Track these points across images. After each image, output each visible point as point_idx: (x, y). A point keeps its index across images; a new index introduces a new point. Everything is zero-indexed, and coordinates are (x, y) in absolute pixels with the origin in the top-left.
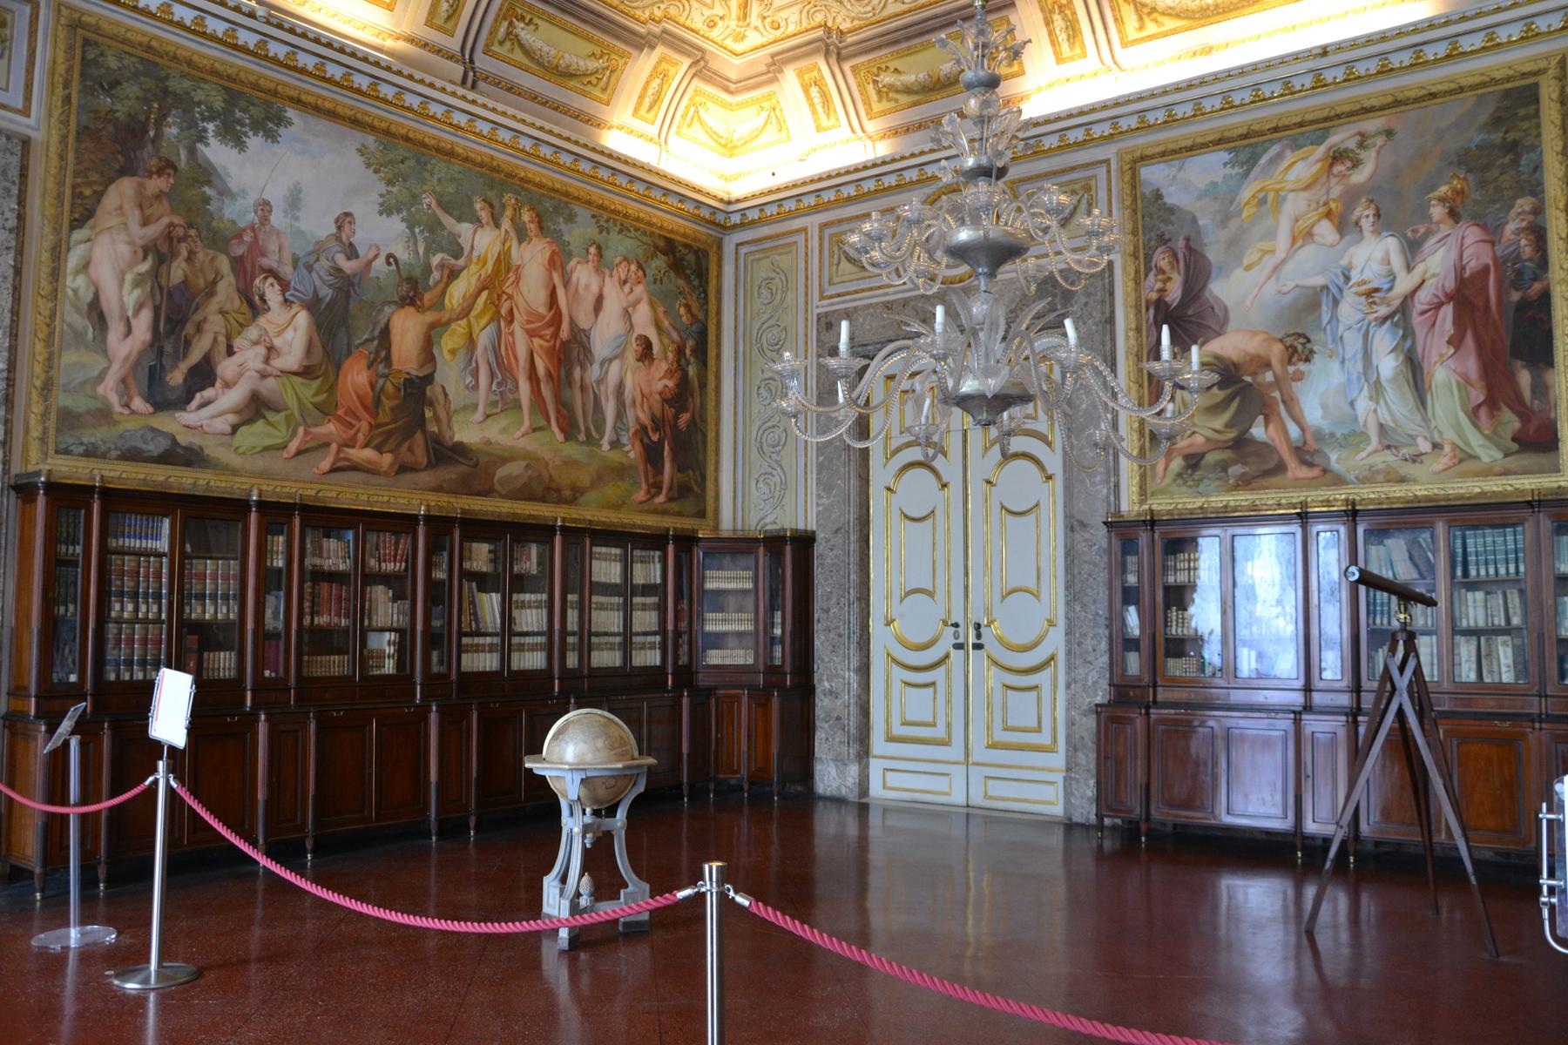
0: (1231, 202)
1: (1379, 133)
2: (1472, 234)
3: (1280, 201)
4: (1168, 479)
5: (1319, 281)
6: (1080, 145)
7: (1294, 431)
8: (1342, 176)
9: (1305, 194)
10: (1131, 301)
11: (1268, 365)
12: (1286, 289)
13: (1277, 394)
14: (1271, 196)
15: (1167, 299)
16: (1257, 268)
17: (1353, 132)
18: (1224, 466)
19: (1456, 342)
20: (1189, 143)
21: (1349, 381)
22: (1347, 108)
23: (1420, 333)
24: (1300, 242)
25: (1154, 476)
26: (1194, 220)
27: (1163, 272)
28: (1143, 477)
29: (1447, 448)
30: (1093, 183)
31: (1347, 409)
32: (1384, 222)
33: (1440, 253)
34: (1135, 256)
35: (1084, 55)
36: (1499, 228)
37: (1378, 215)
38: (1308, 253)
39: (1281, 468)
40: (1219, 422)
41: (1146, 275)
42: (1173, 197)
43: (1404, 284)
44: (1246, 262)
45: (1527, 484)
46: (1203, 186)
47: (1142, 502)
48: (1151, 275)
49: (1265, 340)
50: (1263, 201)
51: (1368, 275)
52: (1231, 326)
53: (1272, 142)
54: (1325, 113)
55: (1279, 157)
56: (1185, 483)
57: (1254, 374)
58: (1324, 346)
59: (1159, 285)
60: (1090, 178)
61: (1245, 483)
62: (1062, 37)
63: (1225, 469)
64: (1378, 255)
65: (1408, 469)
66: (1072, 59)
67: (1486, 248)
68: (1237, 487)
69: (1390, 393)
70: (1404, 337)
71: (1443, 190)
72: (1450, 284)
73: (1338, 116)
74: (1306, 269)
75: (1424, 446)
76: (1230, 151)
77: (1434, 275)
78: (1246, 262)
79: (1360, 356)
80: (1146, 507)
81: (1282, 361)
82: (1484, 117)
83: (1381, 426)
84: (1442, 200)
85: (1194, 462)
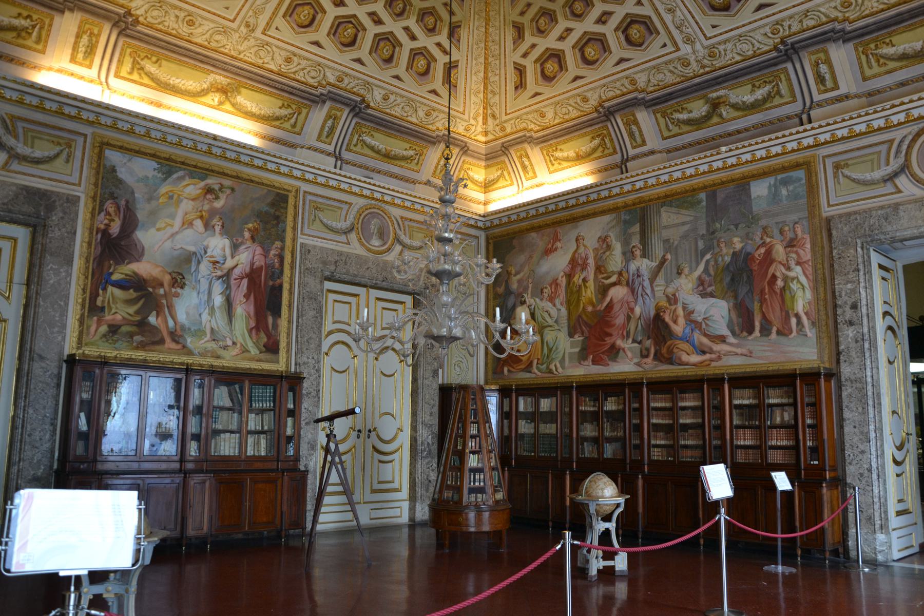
0: (155, 191)
2: (259, 250)
3: (179, 201)
4: (97, 337)
5: (192, 249)
6: (70, 117)
7: (171, 323)
8: (210, 201)
9: (191, 202)
10: (88, 225)
11: (162, 285)
12: (176, 248)
13: (164, 302)
14: (175, 197)
18: (131, 335)
19: (247, 296)
20: (137, 149)
23: (234, 288)
25: (88, 334)
26: (133, 193)
27: (110, 215)
29: (239, 345)
30: (73, 144)
32: (226, 231)
33: (246, 254)
34: (94, 198)
35: (90, 67)
37: (223, 226)
38: (189, 232)
39: (162, 341)
40: (132, 310)
41: (99, 213)
42: (122, 174)
43: (230, 263)
44: (158, 226)
46: (140, 176)
47: (78, 348)
48: (102, 214)
50: (171, 198)
51: (215, 253)
52: (145, 258)
53: (181, 169)
54: (207, 167)
55: (182, 178)
56: (107, 341)
57: (154, 288)
59: (106, 221)
60: (73, 140)
61: (142, 346)
62: (82, 49)
63: (132, 337)
64: (220, 246)
65: (221, 352)
66: (81, 64)
67: (263, 258)
68: (137, 348)
69: (218, 314)
70: (227, 288)
71: (250, 225)
72: (248, 270)
73: (212, 171)
74: (188, 240)
75: (229, 343)
76: (159, 163)
79: (206, 292)
80: (81, 351)
82: (270, 199)
84: (249, 230)
85: (114, 329)
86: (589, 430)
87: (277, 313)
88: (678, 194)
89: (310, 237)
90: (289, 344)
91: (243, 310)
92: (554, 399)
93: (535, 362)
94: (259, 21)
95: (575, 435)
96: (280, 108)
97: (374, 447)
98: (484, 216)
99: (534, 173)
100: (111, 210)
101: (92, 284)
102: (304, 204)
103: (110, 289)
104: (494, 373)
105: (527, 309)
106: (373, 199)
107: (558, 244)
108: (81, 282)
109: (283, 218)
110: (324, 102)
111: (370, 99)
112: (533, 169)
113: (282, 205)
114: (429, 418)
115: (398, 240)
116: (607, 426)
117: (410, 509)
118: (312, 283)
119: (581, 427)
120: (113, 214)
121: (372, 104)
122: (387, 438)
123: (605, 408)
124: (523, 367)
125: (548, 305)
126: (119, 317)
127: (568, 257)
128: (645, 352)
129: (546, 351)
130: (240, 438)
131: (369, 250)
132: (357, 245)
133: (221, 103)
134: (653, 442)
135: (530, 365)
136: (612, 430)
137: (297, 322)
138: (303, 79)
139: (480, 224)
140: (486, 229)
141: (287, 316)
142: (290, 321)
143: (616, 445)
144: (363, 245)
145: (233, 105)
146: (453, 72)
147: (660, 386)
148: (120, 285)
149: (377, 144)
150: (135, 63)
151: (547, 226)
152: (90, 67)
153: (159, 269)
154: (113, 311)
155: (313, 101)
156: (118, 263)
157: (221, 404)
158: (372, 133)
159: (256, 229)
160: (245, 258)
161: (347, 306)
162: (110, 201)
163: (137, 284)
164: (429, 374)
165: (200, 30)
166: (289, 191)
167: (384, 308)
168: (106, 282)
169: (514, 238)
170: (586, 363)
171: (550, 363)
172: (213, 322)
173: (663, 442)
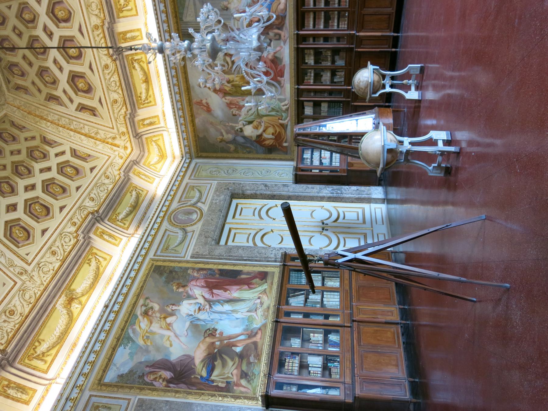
0: (141, 348)
1: (145, 301)
2: (193, 283)
4: (250, 387)
5: (188, 324)
9: (153, 325)
10: (163, 393)
11: (213, 343)
12: (186, 334)
13: (225, 342)
14: (147, 334)
15: (169, 378)
16: (173, 343)
17: (140, 308)
20: (107, 360)
21: (228, 319)
22: (126, 317)
23: (219, 298)
24: (171, 328)
25: (246, 393)
27: (156, 378)
28: (246, 398)
30: (96, 404)
31: (238, 320)
32: (177, 302)
33: (194, 290)
34: (141, 389)
35: (35, 391)
36: (194, 277)
37: (173, 305)
38: (175, 326)
39: (255, 344)
40: (230, 363)
41: (154, 385)
42: (125, 370)
43: (201, 300)
44: (169, 346)
45: (276, 279)
47: (257, 399)
48: (155, 383)
49: (203, 343)
50: (148, 338)
51: (193, 310)
52: (192, 354)
54: (128, 314)
55: (134, 331)
56: (253, 379)
57: (215, 348)
58: (213, 324)
59: (161, 381)
60: (93, 405)
61: (258, 357)
62: (19, 395)
63: (251, 363)
64: (188, 306)
65: (265, 306)
66: (32, 397)
67: (199, 281)
68: (259, 360)
70: (219, 302)
72: (206, 289)
73: (131, 311)
75: (259, 301)
76: (120, 345)
77: (202, 293)
78: (168, 346)
79: (221, 315)
80: (260, 398)
81: (213, 338)
82: (157, 276)
83: (248, 311)
84: (178, 288)
85: (244, 375)
86: (326, 77)
87: (239, 272)
88: (175, 8)
89: (188, 250)
90: (261, 266)
91: (235, 293)
92: (305, 103)
93: (280, 121)
94: (18, 265)
95: (330, 87)
96: (90, 265)
97: (334, 222)
98: (183, 157)
99: (155, 117)
100: (152, 377)
101: (208, 390)
102: (163, 256)
103: (213, 378)
104: (286, 153)
105: (247, 127)
106: (164, 217)
107: (204, 102)
108: (207, 398)
109: (171, 269)
110: (90, 238)
111: (92, 209)
112: (153, 117)
113: (162, 269)
114: (315, 190)
115: (194, 205)
116: (324, 64)
117: (376, 203)
118: (219, 251)
119: (324, 83)
120: (155, 376)
121: (96, 209)
122: (328, 215)
123: (313, 63)
124: (283, 130)
125: (244, 110)
126: (235, 372)
127: (213, 95)
128: (277, 37)
129: (273, 113)
130: (327, 291)
131: (199, 220)
132: (194, 228)
133: (80, 303)
134: (336, 28)
135: (282, 125)
136: (327, 61)
137: (245, 260)
138: (70, 247)
139: (188, 161)
140: (191, 158)
141: (241, 267)
142: (245, 265)
143: (337, 58)
144: (195, 223)
145: (83, 295)
146: (78, 153)
147: (300, 23)
148: (211, 371)
149: (125, 211)
150: (38, 358)
151: (191, 110)
152: (35, 391)
153: (201, 345)
154: (230, 375)
155: (88, 244)
156: (194, 373)
157: (303, 302)
158: (117, 213)
159: (178, 284)
160: (198, 291)
161: (237, 235)
162: (145, 378)
163: (212, 359)
164: (286, 189)
165: (19, 308)
166: (152, 265)
167: (240, 214)
168: (208, 380)
169: (198, 136)
170: (282, 82)
171: (282, 110)
172: (242, 311)
173: (336, 21)
